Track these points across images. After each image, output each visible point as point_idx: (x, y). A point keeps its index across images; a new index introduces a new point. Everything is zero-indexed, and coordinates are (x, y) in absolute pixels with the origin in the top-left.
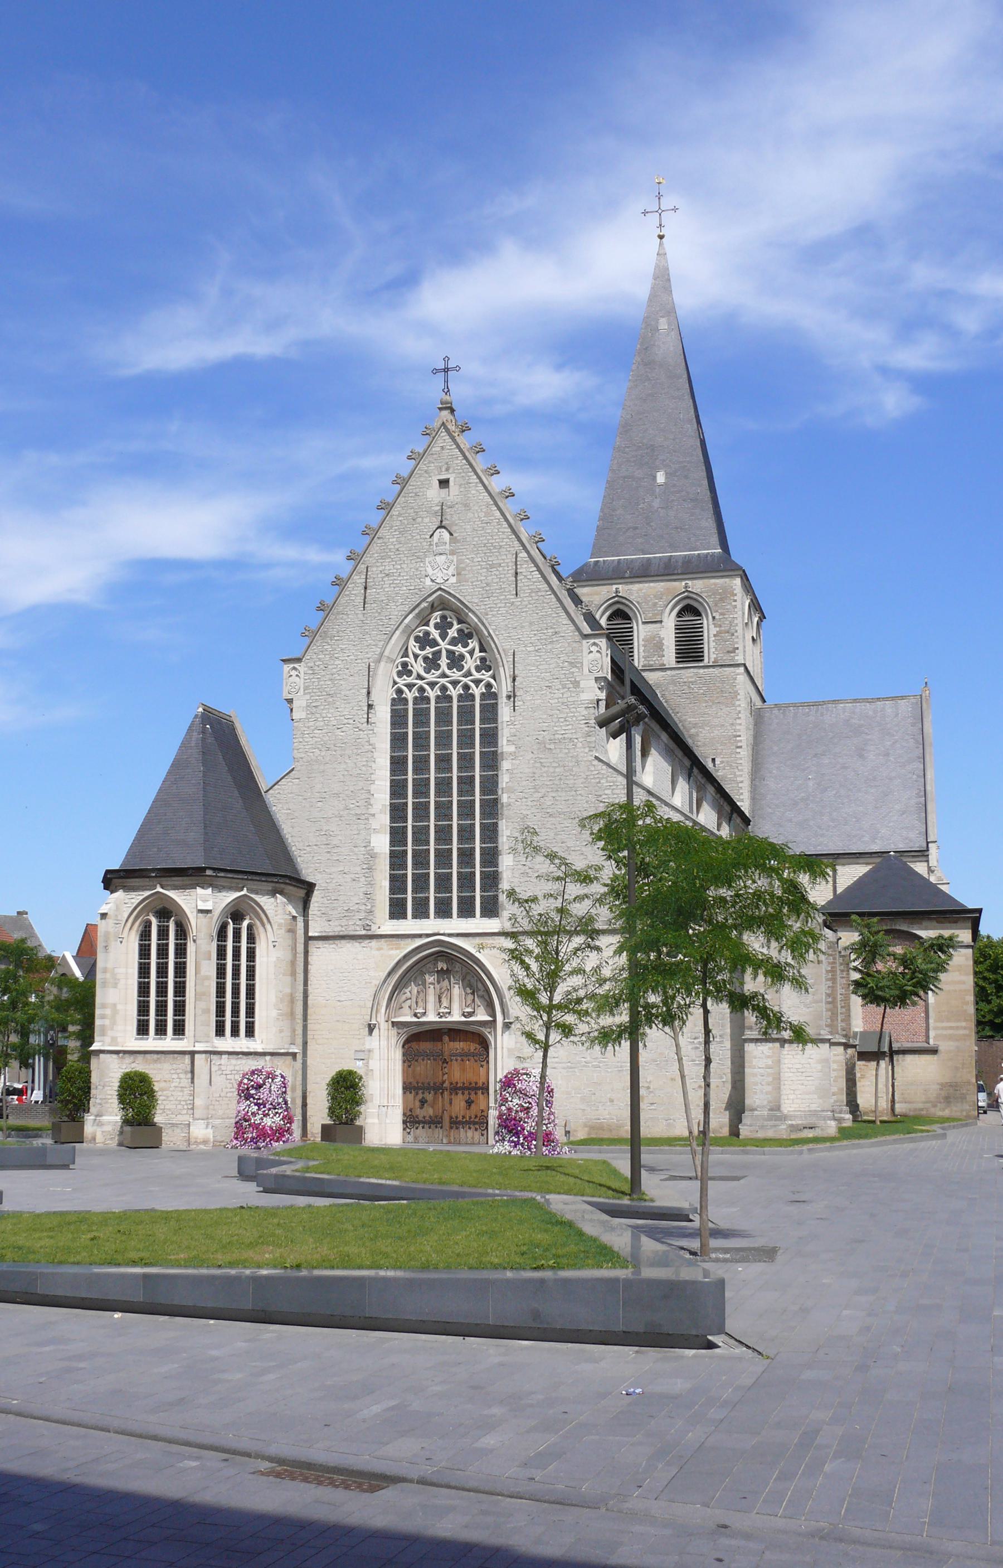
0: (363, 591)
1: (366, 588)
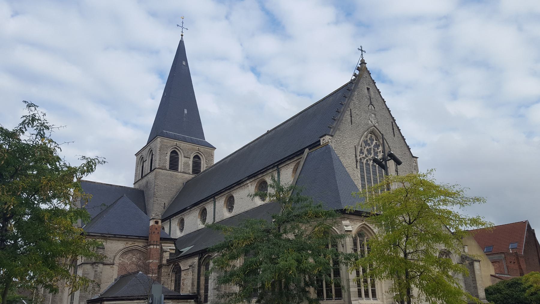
0: (350, 118)
1: (351, 117)
